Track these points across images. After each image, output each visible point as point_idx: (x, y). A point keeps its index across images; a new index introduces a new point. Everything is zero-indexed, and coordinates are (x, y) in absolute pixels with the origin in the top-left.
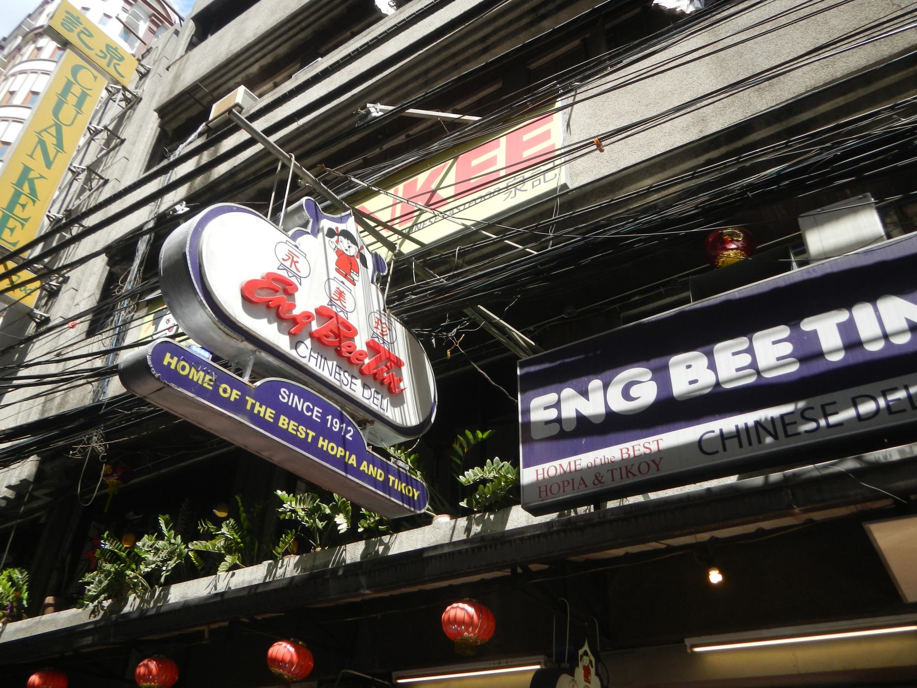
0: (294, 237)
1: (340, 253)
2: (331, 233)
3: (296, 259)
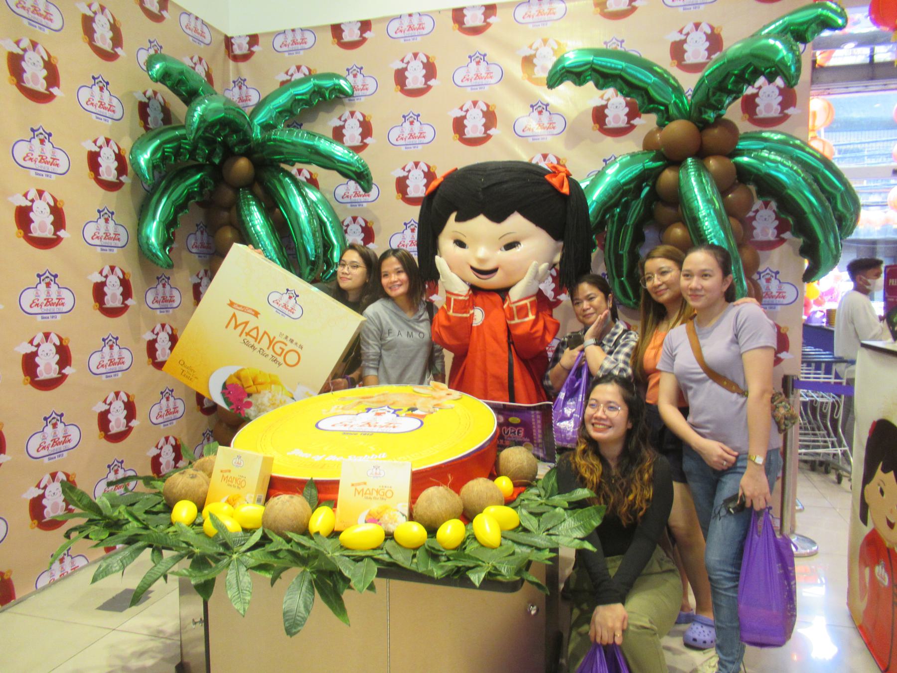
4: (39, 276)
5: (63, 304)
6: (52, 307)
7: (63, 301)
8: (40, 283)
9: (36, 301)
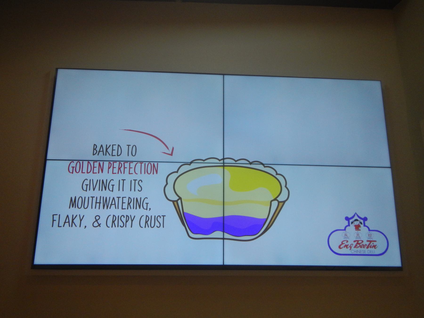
0: (345, 230)
1: (355, 226)
2: (352, 223)
3: (346, 234)
4: (347, 219)
5: (375, 246)
6: (362, 249)
8: (349, 225)
9: (345, 242)
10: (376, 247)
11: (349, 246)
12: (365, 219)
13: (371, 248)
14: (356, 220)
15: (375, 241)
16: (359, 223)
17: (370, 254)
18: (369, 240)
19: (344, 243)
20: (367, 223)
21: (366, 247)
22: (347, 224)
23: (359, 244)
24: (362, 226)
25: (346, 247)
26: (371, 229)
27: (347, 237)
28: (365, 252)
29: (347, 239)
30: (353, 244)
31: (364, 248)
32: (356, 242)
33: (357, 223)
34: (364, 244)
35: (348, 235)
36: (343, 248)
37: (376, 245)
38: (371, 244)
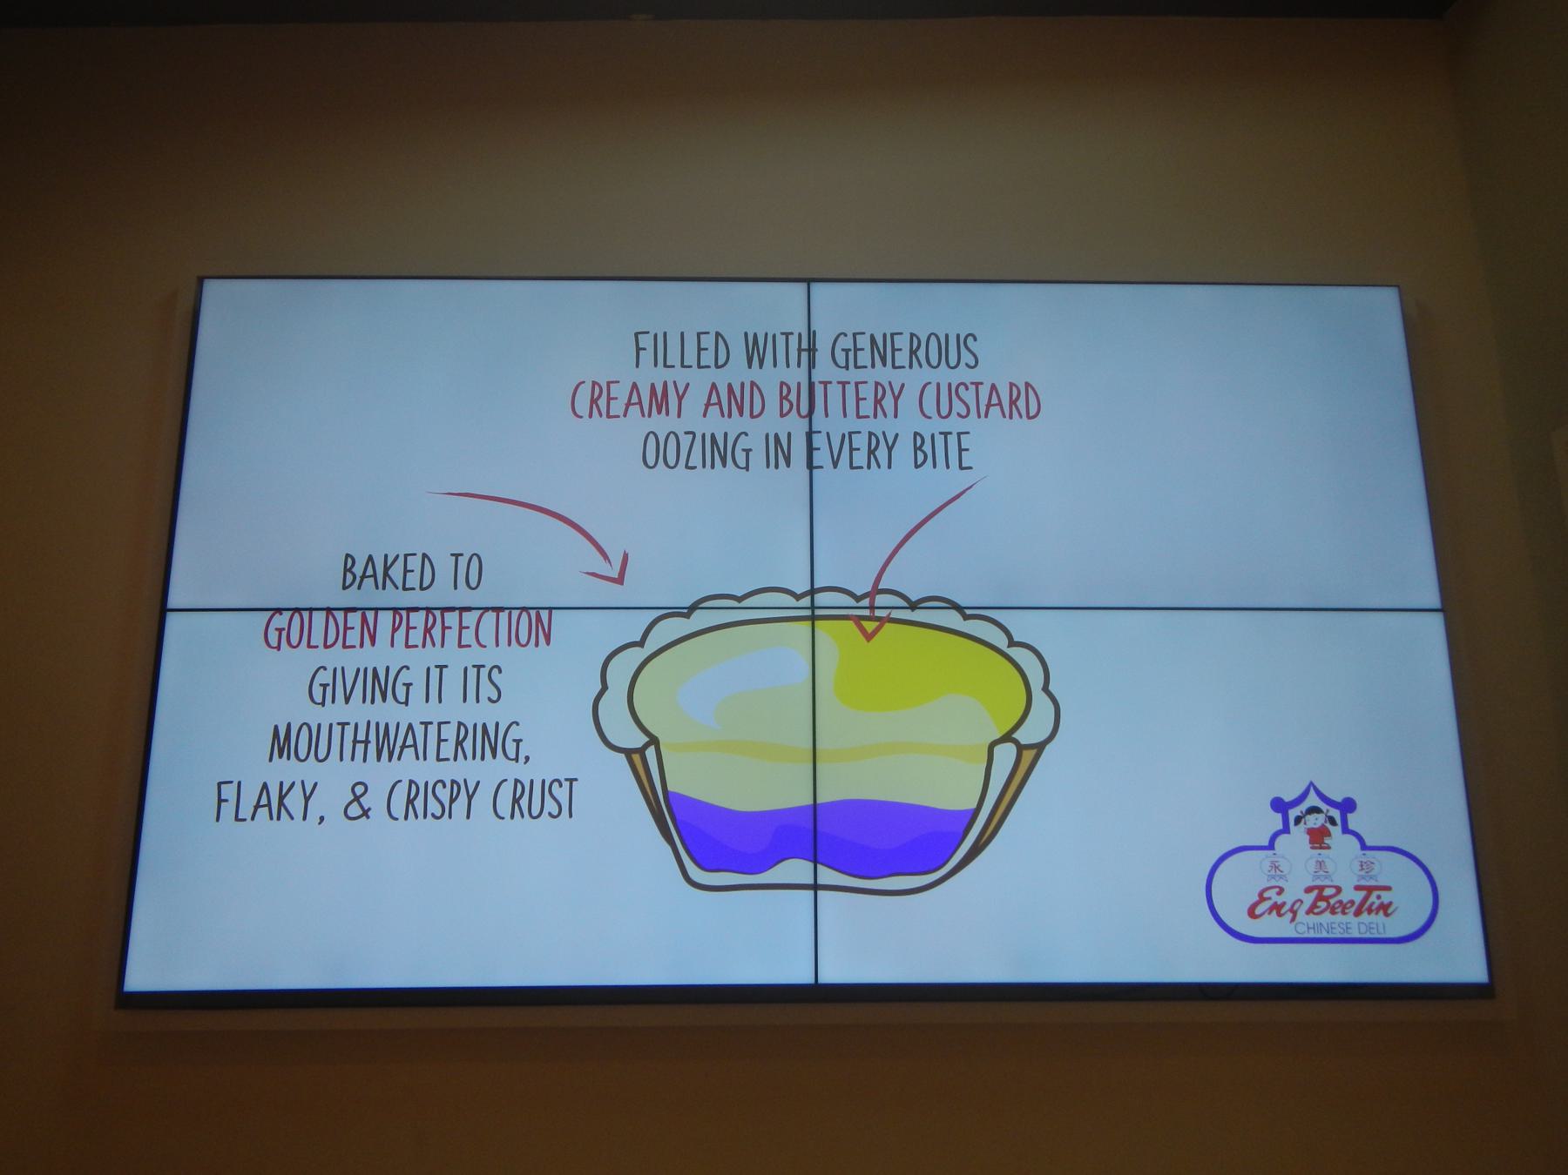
0: (1271, 846)
1: (1310, 832)
2: (1298, 820)
4: (1279, 806)
5: (1385, 908)
6: (1339, 918)
7: (1386, 897)
8: (1286, 830)
10: (1389, 912)
11: (1287, 907)
12: (1348, 806)
13: (1373, 915)
14: (1314, 810)
15: (1388, 888)
16: (1326, 822)
17: (1368, 935)
18: (1363, 883)
19: (1269, 898)
20: (1354, 821)
21: (1353, 909)
22: (1280, 826)
23: (1327, 899)
24: (1336, 831)
25: (1274, 912)
26: (1369, 843)
27: (1278, 872)
28: (1349, 930)
29: (1280, 884)
30: (1302, 902)
31: (1344, 913)
32: (1315, 893)
33: (1315, 821)
34: (1345, 901)
35: (1284, 866)
36: (1266, 914)
37: (1390, 904)
38: (1372, 899)
